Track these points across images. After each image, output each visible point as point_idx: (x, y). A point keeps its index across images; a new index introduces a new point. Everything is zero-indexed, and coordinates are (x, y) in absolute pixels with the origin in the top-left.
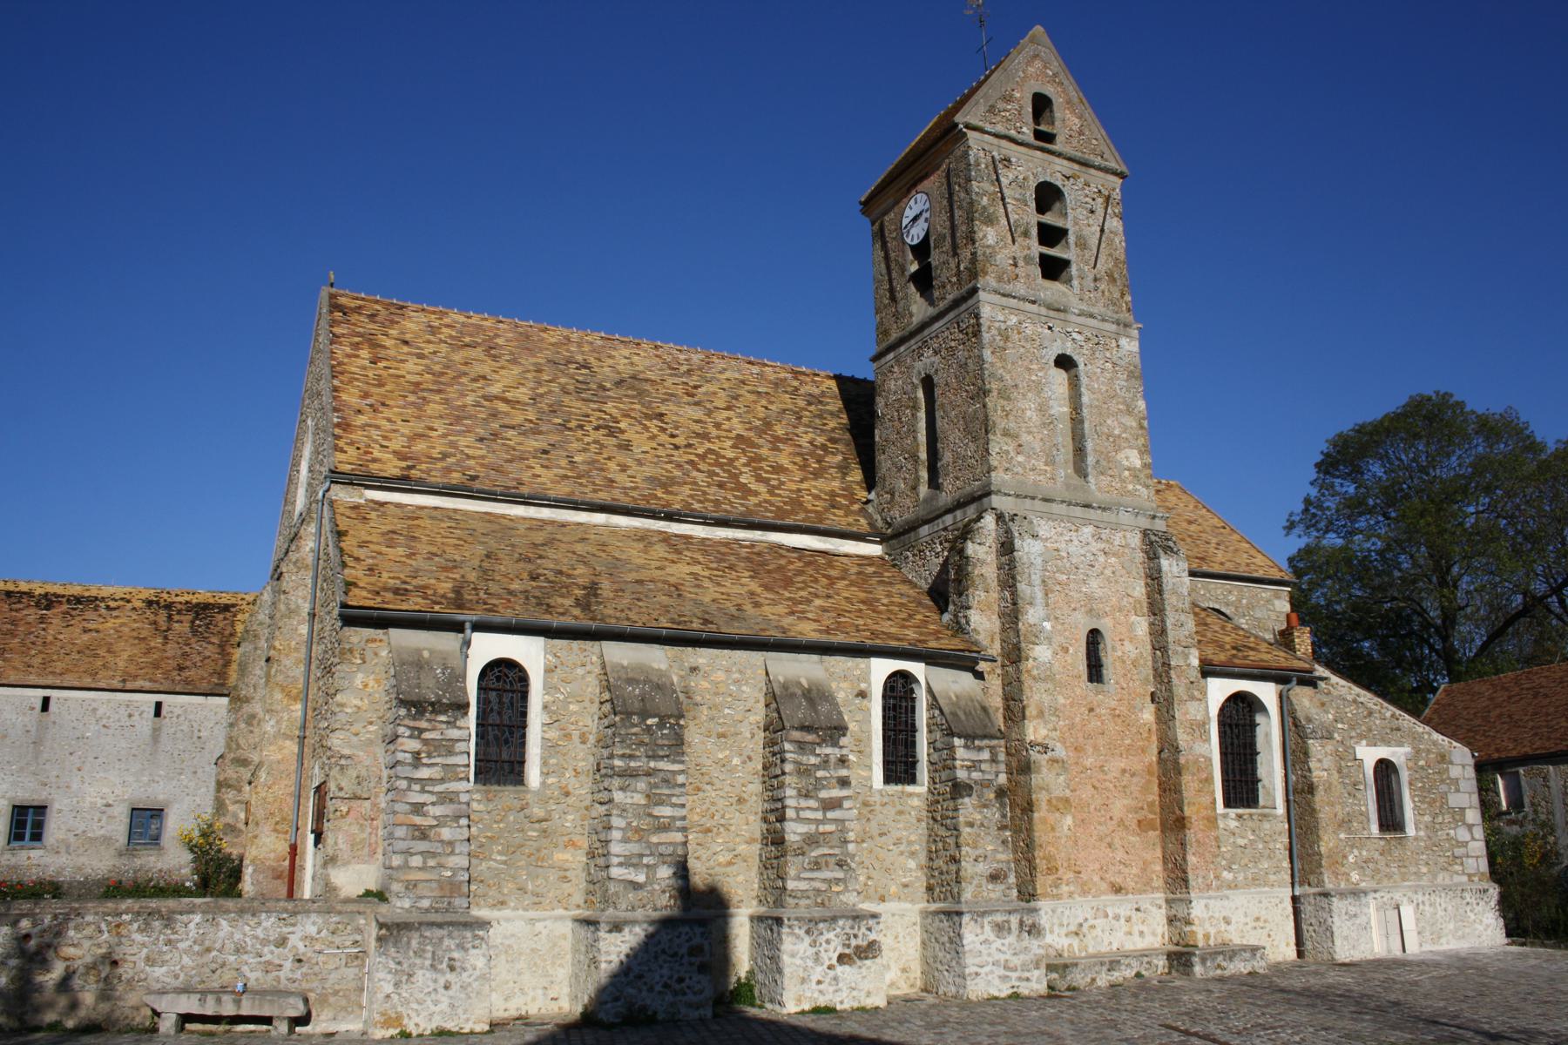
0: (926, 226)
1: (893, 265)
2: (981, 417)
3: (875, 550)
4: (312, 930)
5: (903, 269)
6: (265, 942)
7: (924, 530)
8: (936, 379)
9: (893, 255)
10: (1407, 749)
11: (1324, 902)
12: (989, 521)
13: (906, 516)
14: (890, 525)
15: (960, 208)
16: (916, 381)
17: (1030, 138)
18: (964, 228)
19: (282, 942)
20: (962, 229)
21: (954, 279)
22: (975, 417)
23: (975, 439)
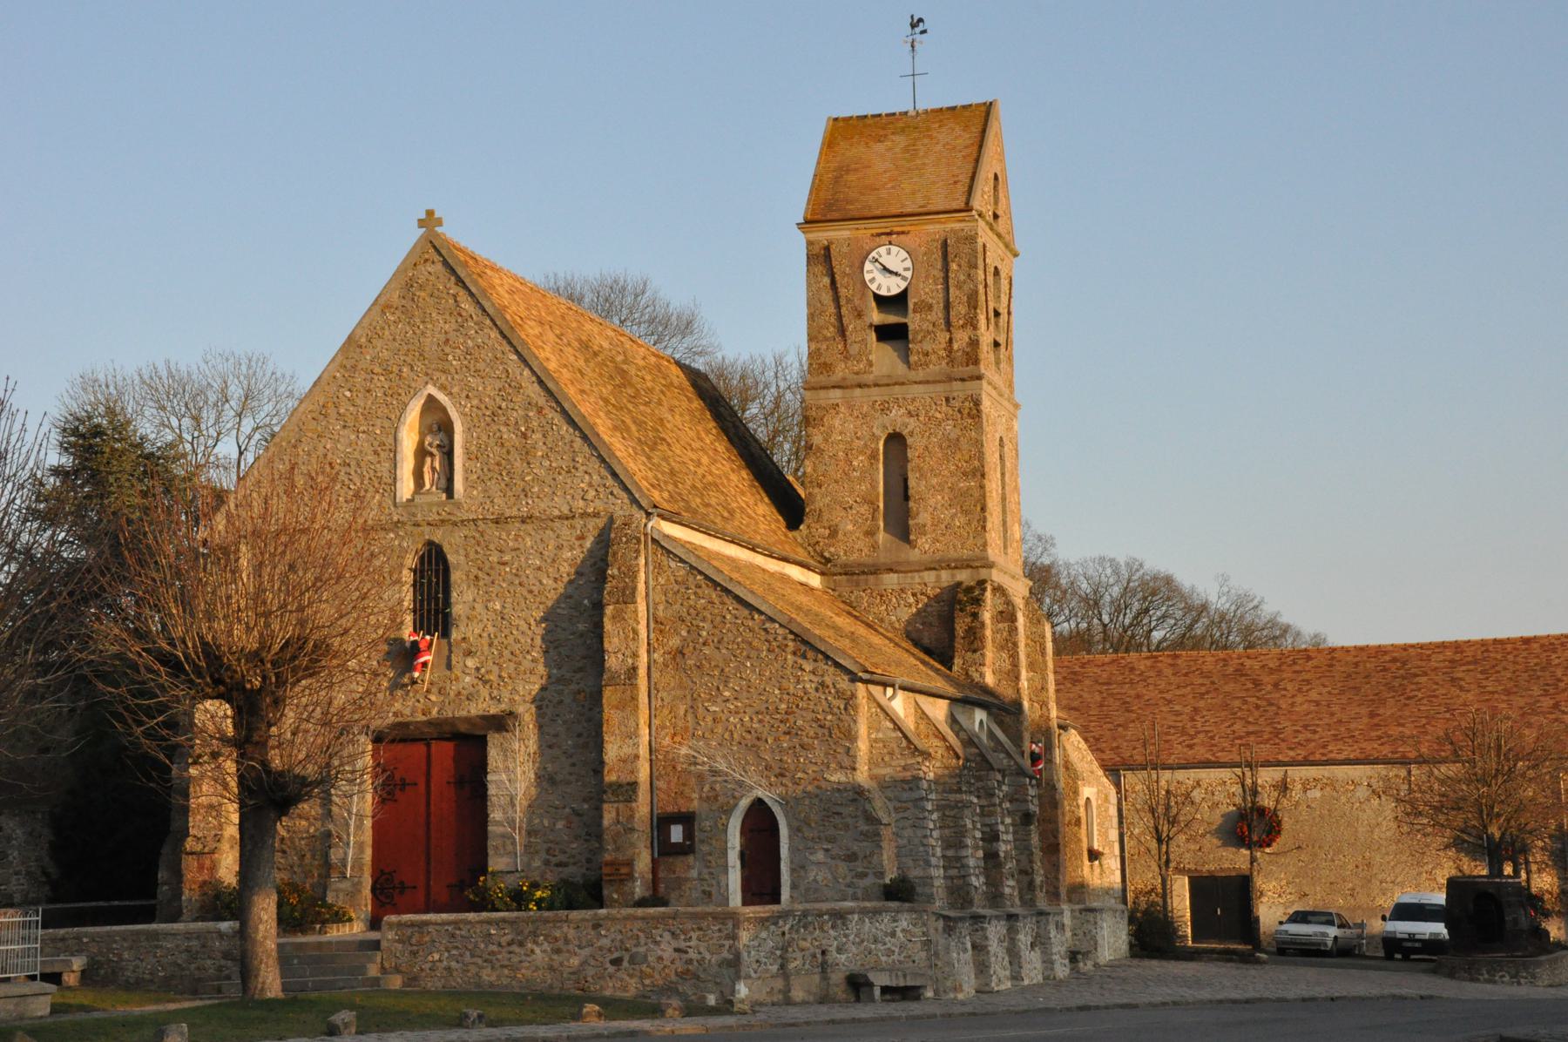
0: (903, 285)
1: (843, 302)
2: (976, 495)
3: (815, 580)
4: (905, 924)
5: (860, 315)
6: (886, 934)
7: (891, 580)
8: (910, 441)
9: (843, 292)
10: (1095, 790)
11: (1091, 917)
12: (988, 594)
13: (854, 557)
14: (828, 560)
15: (959, 287)
16: (877, 432)
17: (991, 219)
18: (963, 309)
19: (893, 934)
20: (959, 309)
21: (943, 353)
22: (965, 493)
23: (966, 513)
